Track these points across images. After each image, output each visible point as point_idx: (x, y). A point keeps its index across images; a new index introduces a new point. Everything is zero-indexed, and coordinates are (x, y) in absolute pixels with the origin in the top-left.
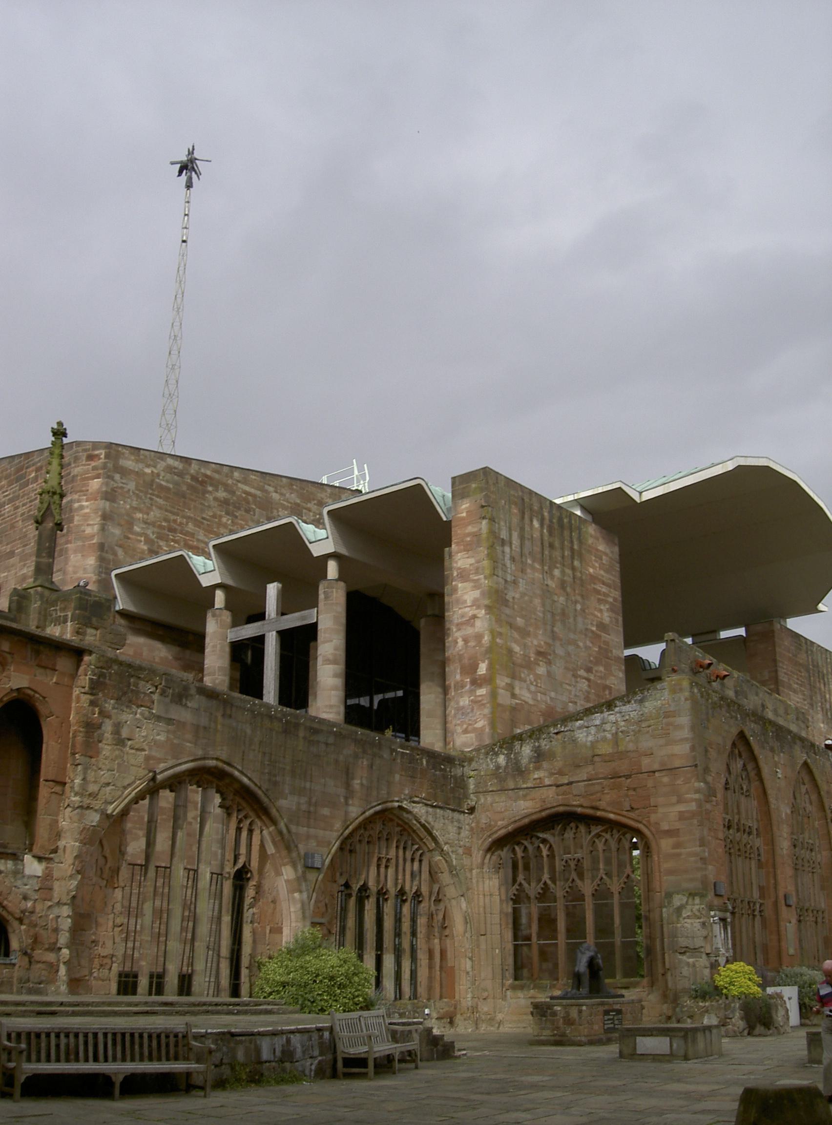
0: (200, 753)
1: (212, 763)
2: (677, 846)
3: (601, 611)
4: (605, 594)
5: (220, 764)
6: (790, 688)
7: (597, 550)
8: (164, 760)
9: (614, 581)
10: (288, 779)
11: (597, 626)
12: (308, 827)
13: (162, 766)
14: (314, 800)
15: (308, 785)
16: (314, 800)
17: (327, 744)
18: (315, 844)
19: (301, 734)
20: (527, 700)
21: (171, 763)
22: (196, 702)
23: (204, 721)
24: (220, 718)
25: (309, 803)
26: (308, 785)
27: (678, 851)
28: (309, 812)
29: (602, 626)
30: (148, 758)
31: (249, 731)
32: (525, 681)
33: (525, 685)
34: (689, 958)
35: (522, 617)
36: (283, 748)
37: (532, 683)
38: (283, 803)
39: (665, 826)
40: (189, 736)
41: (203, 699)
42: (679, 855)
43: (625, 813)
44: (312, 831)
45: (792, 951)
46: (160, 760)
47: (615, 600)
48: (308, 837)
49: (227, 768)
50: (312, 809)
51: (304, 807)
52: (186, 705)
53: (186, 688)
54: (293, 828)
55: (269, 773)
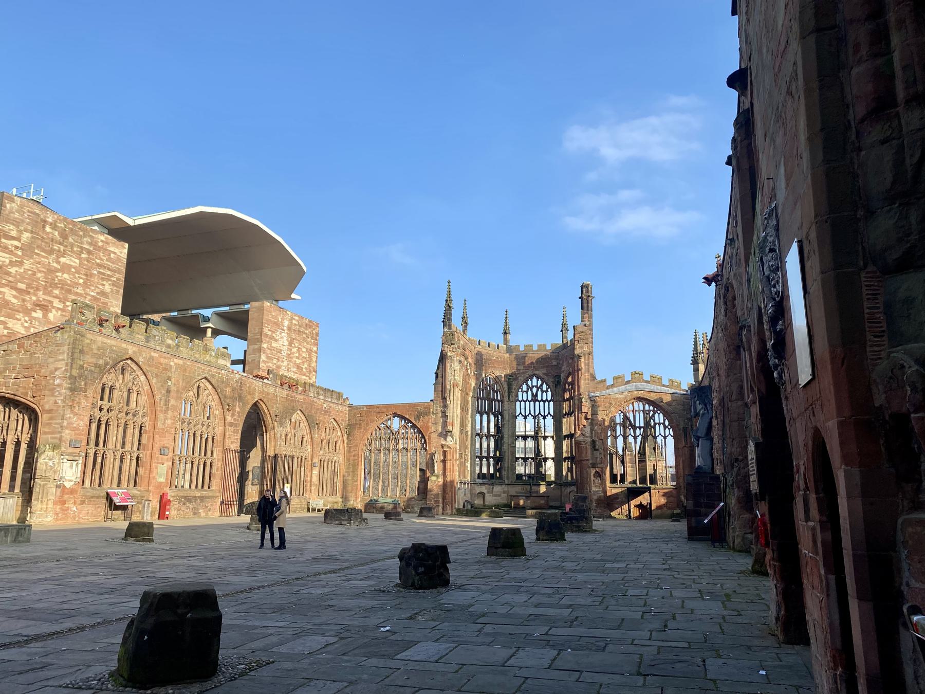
2: (51, 418)
3: (104, 285)
4: (108, 275)
6: (272, 338)
7: (107, 250)
9: (119, 269)
11: (98, 293)
20: (19, 331)
27: (51, 421)
29: (103, 293)
32: (20, 320)
33: (19, 322)
34: (42, 481)
35: (24, 283)
37: (26, 321)
39: (47, 407)
42: (51, 423)
43: (29, 399)
45: (162, 480)
47: (118, 279)
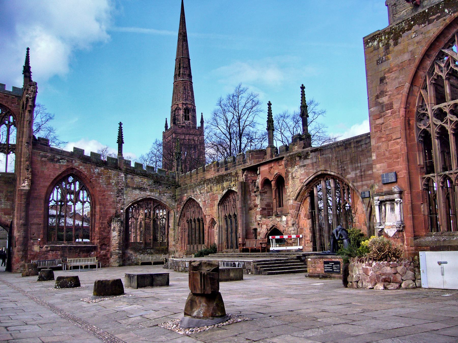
0: (315, 171)
1: (319, 173)
5: (323, 172)
8: (305, 178)
10: (350, 166)
12: (362, 181)
13: (304, 180)
14: (363, 170)
15: (359, 165)
16: (363, 170)
17: (366, 144)
18: (366, 187)
19: (352, 146)
21: (307, 179)
22: (312, 155)
23: (314, 160)
24: (320, 157)
25: (361, 172)
26: (359, 165)
28: (361, 175)
30: (300, 180)
31: (330, 156)
36: (345, 156)
38: (349, 176)
40: (311, 168)
41: (313, 153)
44: (364, 183)
46: (303, 179)
48: (362, 186)
49: (325, 172)
50: (363, 174)
51: (359, 174)
52: (308, 159)
53: (307, 153)
54: (355, 184)
55: (341, 167)
